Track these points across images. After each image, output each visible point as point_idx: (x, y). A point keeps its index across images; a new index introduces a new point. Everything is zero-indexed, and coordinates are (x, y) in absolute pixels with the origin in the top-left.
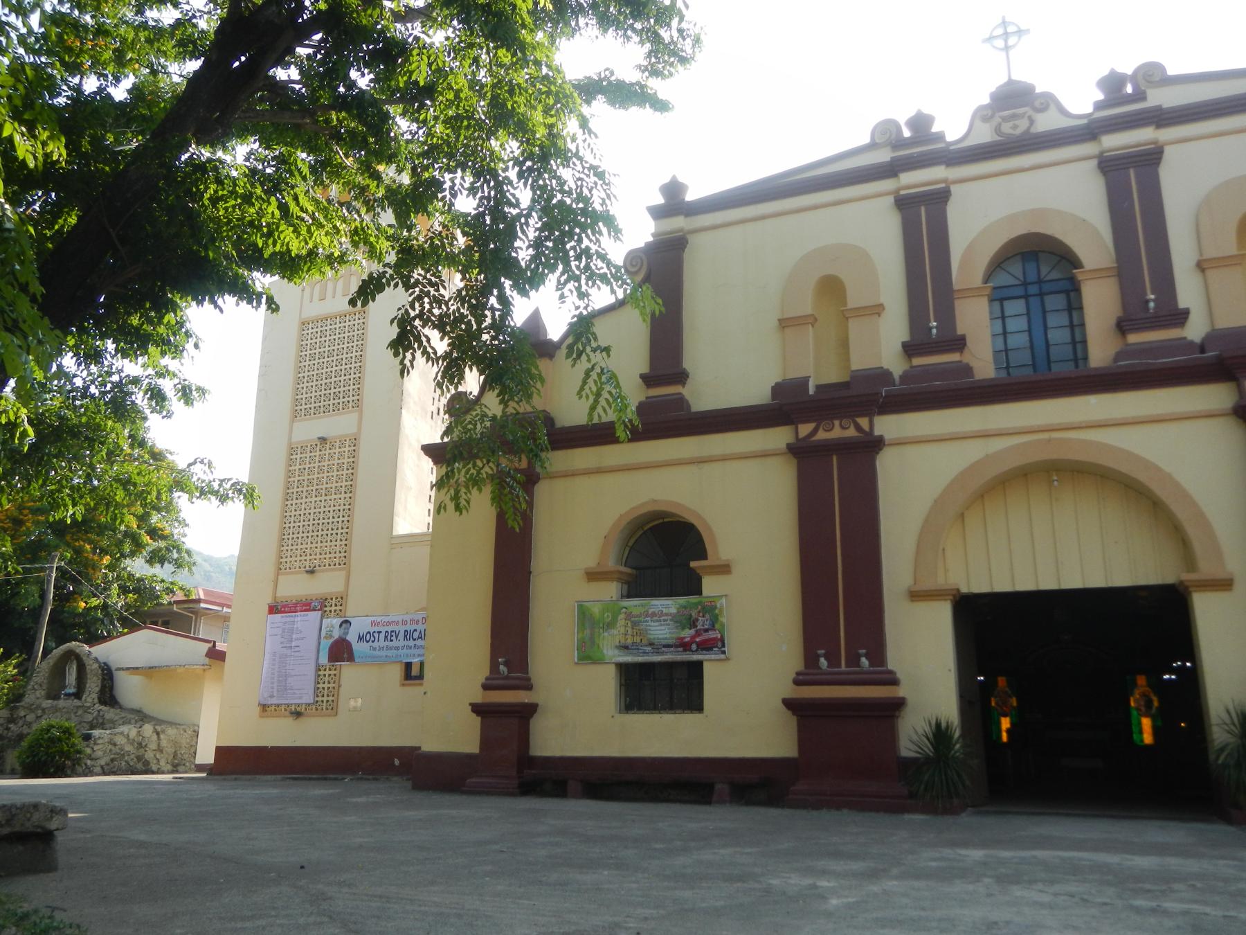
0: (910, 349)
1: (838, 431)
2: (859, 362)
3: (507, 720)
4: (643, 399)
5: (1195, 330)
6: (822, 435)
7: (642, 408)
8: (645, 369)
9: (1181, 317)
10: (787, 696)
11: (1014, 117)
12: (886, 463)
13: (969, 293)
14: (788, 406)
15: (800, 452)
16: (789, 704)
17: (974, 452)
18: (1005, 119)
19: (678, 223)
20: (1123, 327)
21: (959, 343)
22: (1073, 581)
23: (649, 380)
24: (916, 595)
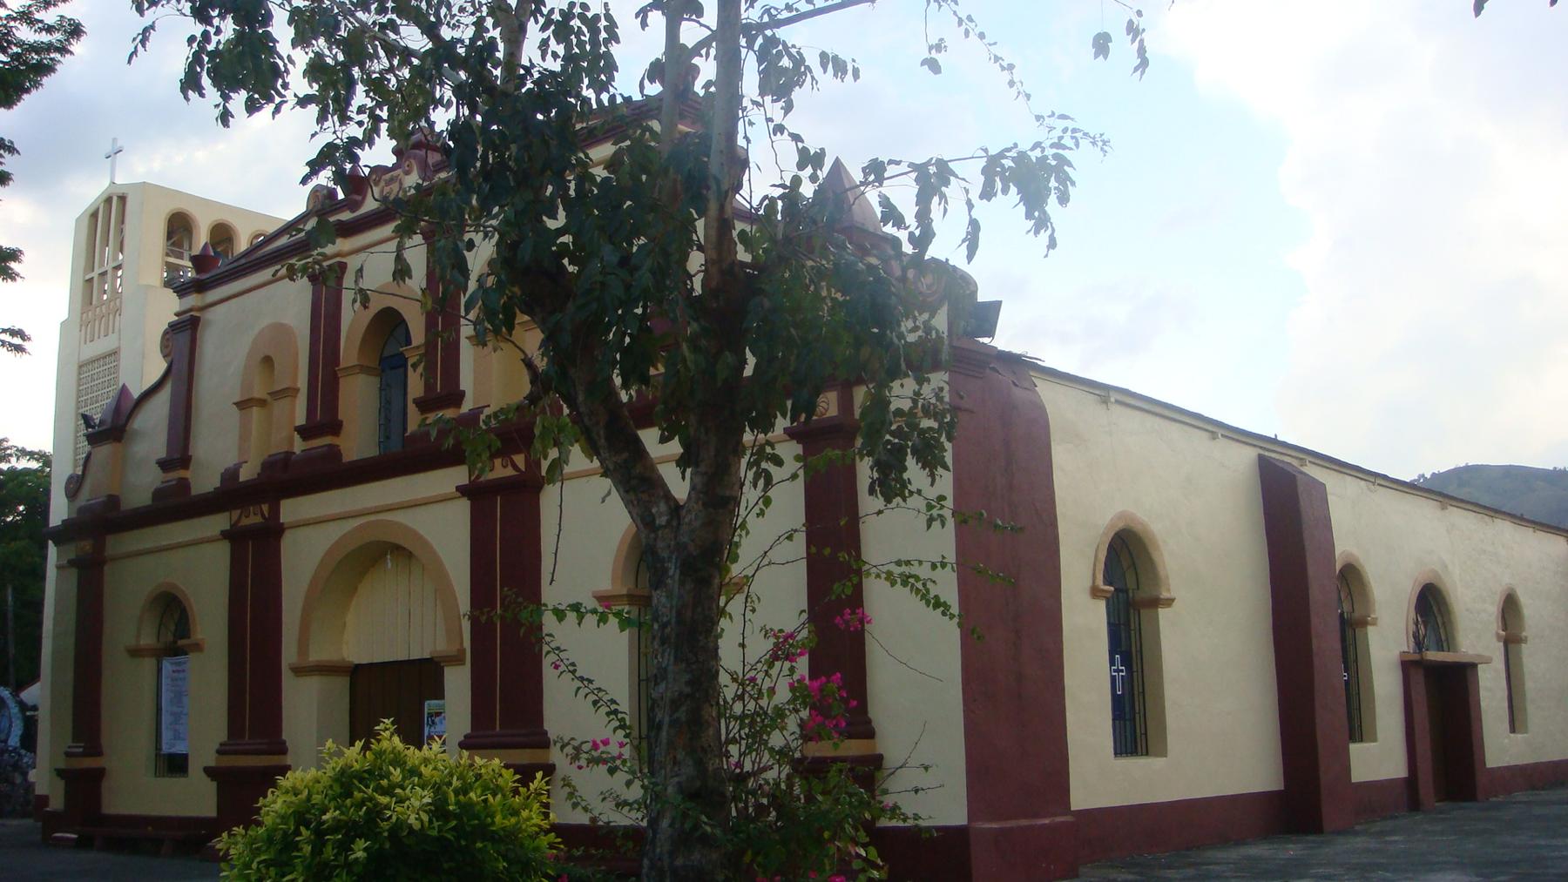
0: (305, 432)
1: (253, 519)
2: (277, 446)
3: (84, 784)
4: (158, 484)
5: (466, 407)
6: (245, 522)
7: (158, 494)
8: (162, 453)
9: (457, 398)
10: (212, 764)
11: (392, 180)
12: (288, 543)
13: (349, 370)
14: (231, 494)
15: (234, 536)
16: (210, 772)
17: (332, 534)
18: (388, 183)
19: (193, 300)
20: (424, 405)
21: (335, 427)
22: (415, 656)
23: (165, 465)
24: (299, 671)
